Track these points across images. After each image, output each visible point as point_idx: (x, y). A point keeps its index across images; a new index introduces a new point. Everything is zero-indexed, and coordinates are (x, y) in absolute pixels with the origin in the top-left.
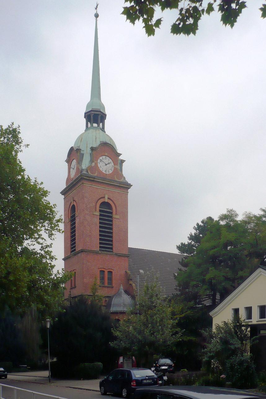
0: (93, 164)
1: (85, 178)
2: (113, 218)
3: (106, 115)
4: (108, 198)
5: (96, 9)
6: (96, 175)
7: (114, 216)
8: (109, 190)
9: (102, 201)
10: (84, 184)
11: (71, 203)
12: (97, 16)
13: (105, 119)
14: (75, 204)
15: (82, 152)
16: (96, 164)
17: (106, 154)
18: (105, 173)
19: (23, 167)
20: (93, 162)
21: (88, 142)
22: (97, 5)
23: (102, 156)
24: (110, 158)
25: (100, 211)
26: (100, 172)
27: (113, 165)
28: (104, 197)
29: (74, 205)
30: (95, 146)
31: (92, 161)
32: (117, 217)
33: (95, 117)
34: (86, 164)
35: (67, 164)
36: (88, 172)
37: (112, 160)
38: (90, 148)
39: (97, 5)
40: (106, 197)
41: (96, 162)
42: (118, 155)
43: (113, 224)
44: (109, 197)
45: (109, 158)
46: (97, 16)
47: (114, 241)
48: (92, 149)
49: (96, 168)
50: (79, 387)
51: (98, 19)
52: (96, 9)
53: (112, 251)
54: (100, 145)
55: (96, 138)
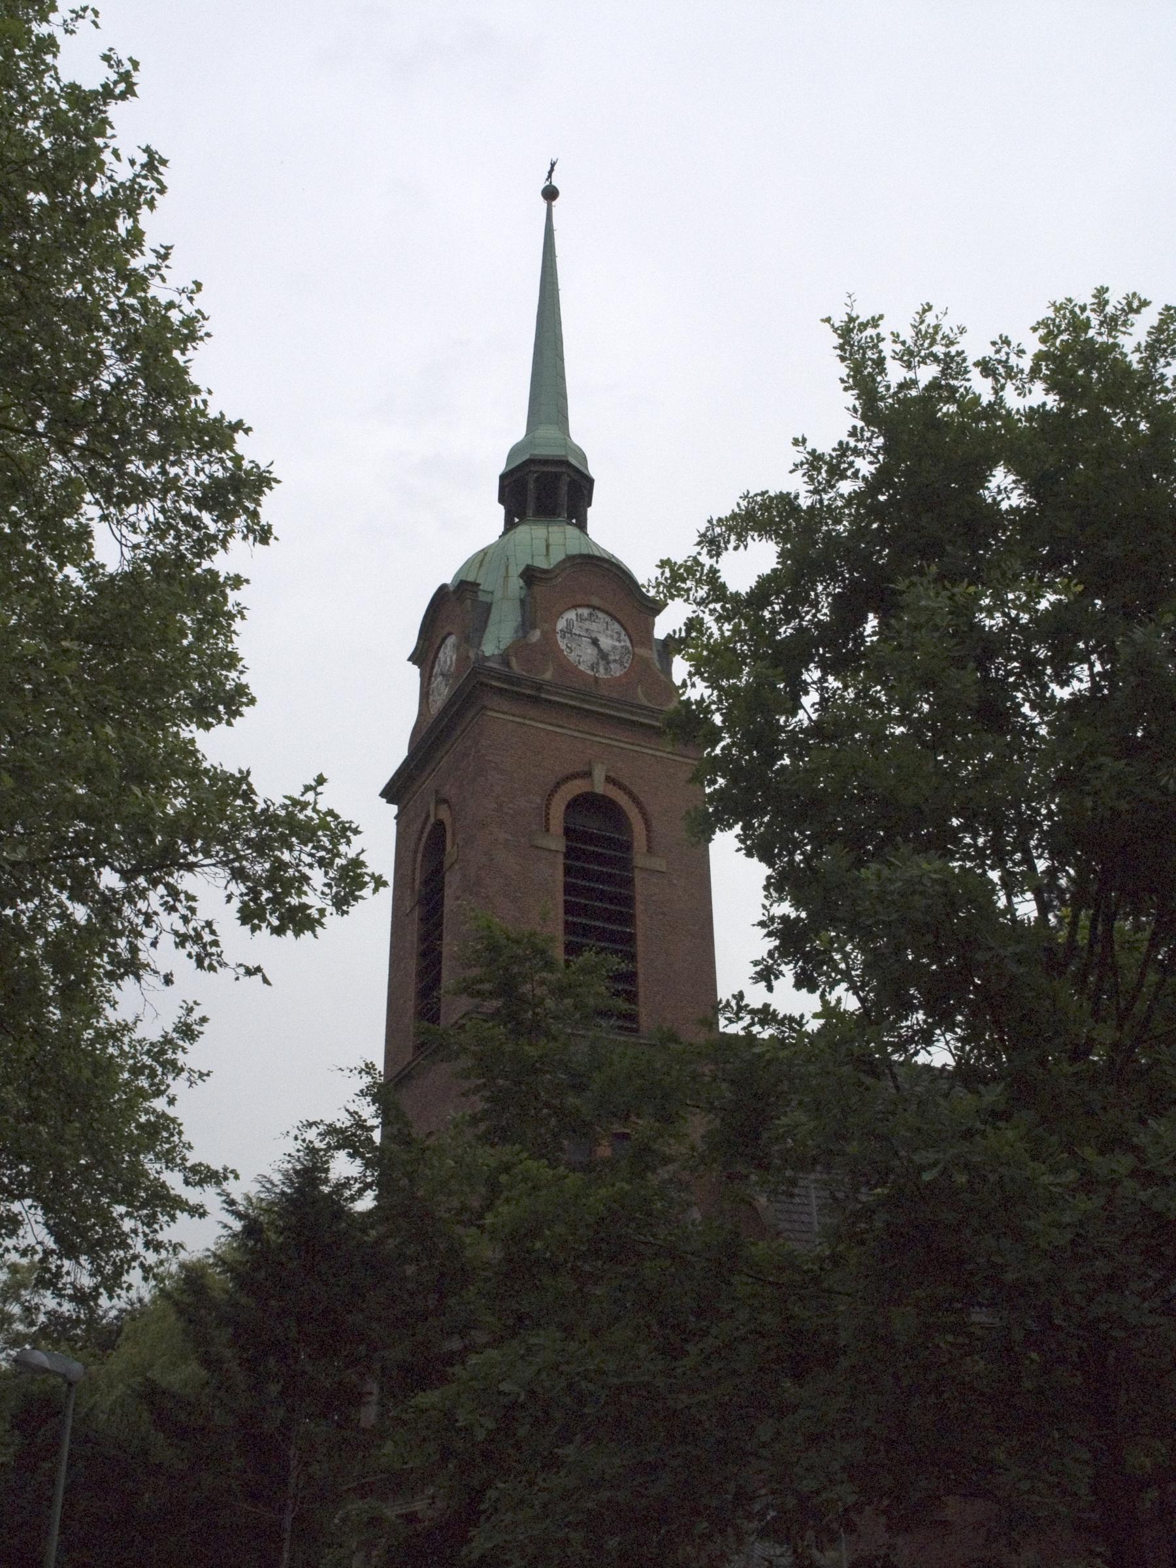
0: (536, 635)
1: (494, 683)
2: (636, 871)
3: (591, 481)
4: (609, 779)
5: (550, 176)
6: (548, 676)
7: (640, 859)
8: (613, 743)
9: (577, 787)
10: (490, 713)
11: (428, 816)
12: (550, 194)
13: (589, 505)
14: (444, 814)
15: (482, 597)
16: (549, 637)
17: (595, 601)
18: (589, 672)
19: (173, 1218)
20: (534, 626)
21: (512, 560)
22: (553, 165)
23: (575, 607)
24: (614, 618)
25: (568, 832)
26: (567, 669)
27: (628, 644)
28: (588, 774)
29: (440, 824)
30: (541, 563)
31: (527, 625)
32: (659, 864)
33: (546, 484)
34: (498, 637)
35: (415, 671)
36: (508, 664)
37: (622, 625)
38: (522, 576)
39: (553, 165)
40: (599, 773)
41: (546, 626)
42: (651, 608)
43: (635, 934)
44: (612, 774)
45: (608, 619)
46: (550, 194)
47: (641, 978)
48: (531, 576)
49: (548, 648)
50: (438, 642)
51: (554, 203)
52: (550, 176)
53: (637, 1031)
54: (564, 561)
55: (548, 546)
